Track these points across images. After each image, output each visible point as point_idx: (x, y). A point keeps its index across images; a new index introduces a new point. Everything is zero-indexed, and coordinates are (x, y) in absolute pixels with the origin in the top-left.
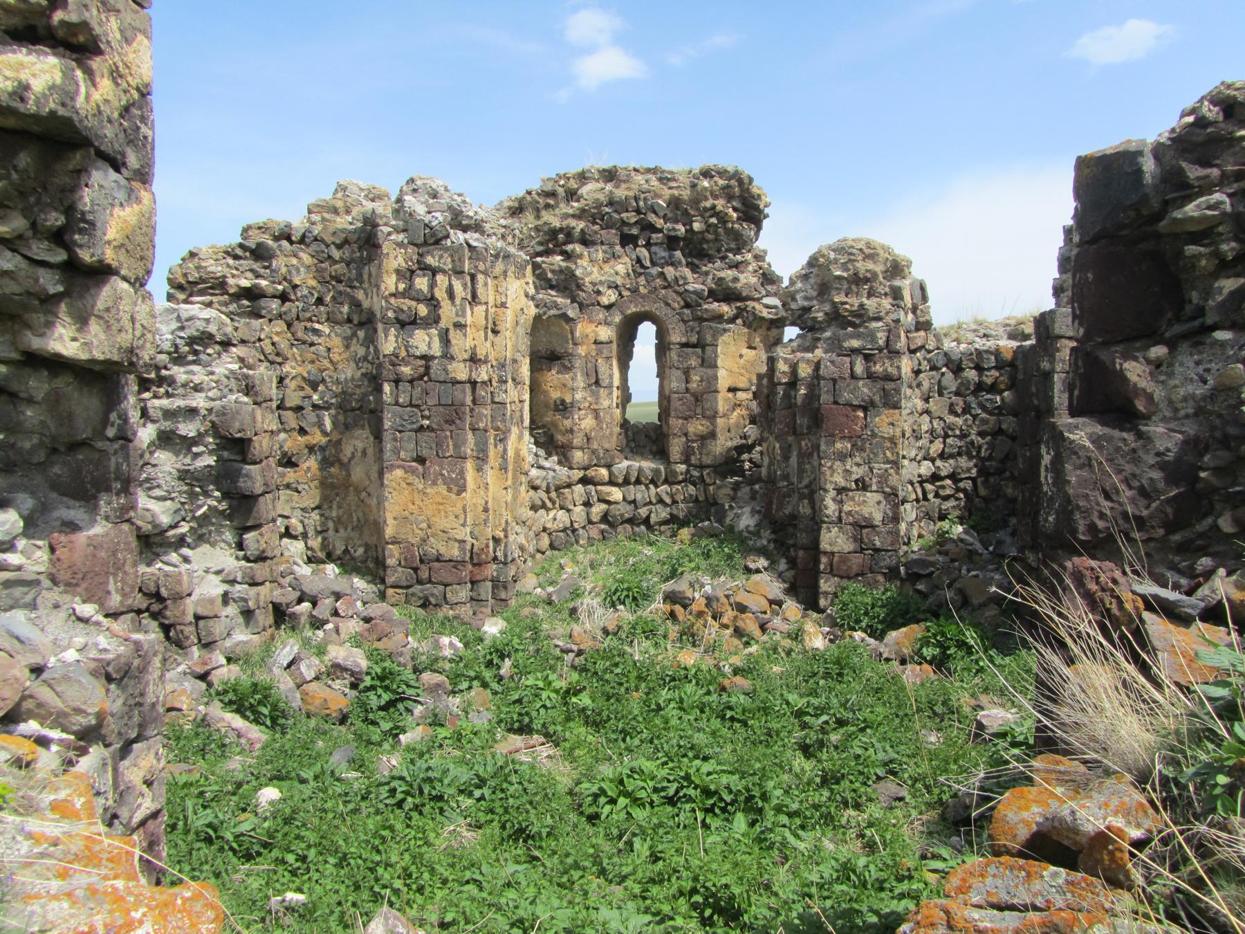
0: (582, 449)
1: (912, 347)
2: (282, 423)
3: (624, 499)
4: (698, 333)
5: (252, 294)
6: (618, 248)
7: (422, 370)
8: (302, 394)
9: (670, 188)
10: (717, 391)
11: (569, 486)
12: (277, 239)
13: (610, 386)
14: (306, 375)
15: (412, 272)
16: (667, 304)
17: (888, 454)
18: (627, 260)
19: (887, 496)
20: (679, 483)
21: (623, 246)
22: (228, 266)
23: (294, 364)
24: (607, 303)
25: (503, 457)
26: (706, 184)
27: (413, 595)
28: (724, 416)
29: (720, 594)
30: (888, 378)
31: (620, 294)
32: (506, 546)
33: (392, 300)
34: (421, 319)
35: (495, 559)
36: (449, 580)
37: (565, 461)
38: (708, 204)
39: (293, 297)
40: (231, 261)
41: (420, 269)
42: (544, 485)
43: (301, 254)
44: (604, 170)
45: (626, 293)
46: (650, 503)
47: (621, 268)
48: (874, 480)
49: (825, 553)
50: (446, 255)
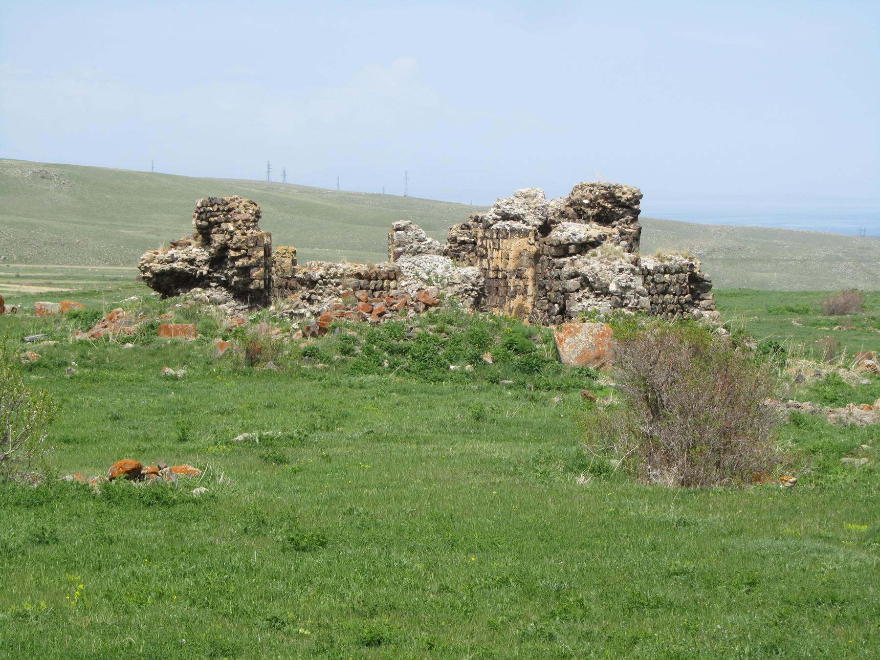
22: (458, 232)
40: (460, 231)
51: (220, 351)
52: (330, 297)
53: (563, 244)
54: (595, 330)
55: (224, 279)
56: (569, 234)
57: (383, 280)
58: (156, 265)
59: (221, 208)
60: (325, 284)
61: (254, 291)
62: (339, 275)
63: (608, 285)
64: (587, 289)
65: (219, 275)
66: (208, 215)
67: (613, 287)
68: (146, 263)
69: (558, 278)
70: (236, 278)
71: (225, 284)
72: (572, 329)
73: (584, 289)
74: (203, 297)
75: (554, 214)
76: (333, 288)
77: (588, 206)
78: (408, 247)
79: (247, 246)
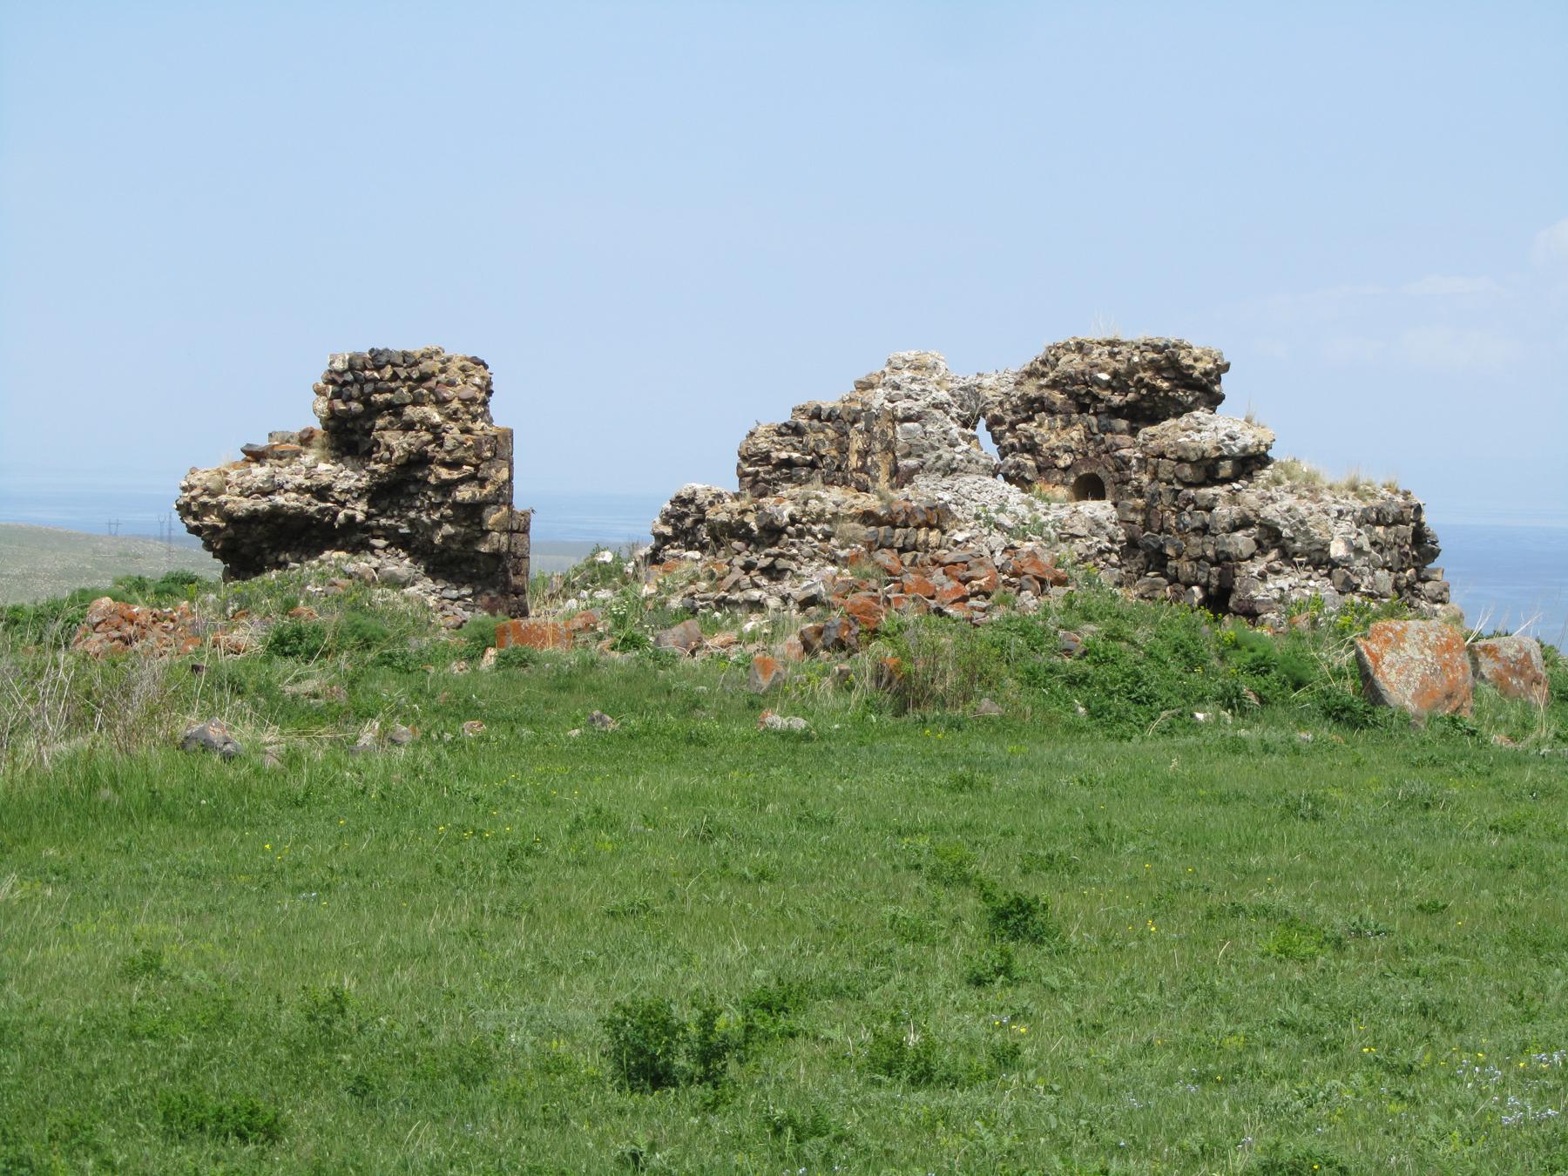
5: (788, 463)
6: (1075, 416)
21: (1079, 413)
22: (773, 442)
40: (776, 439)
43: (827, 430)
47: (1075, 434)
51: (761, 677)
52: (815, 564)
53: (1208, 458)
54: (1432, 637)
55: (405, 530)
56: (1221, 435)
57: (918, 527)
58: (235, 498)
59: (403, 374)
60: (800, 534)
61: (481, 558)
62: (829, 516)
63: (1327, 545)
64: (1273, 554)
65: (392, 522)
66: (368, 388)
67: (1337, 550)
68: (202, 495)
69: (1204, 530)
70: (448, 529)
71: (412, 544)
72: (1391, 635)
73: (1265, 553)
74: (366, 571)
75: (1001, 403)
76: (816, 543)
77: (1108, 385)
78: (930, 457)
79: (478, 457)
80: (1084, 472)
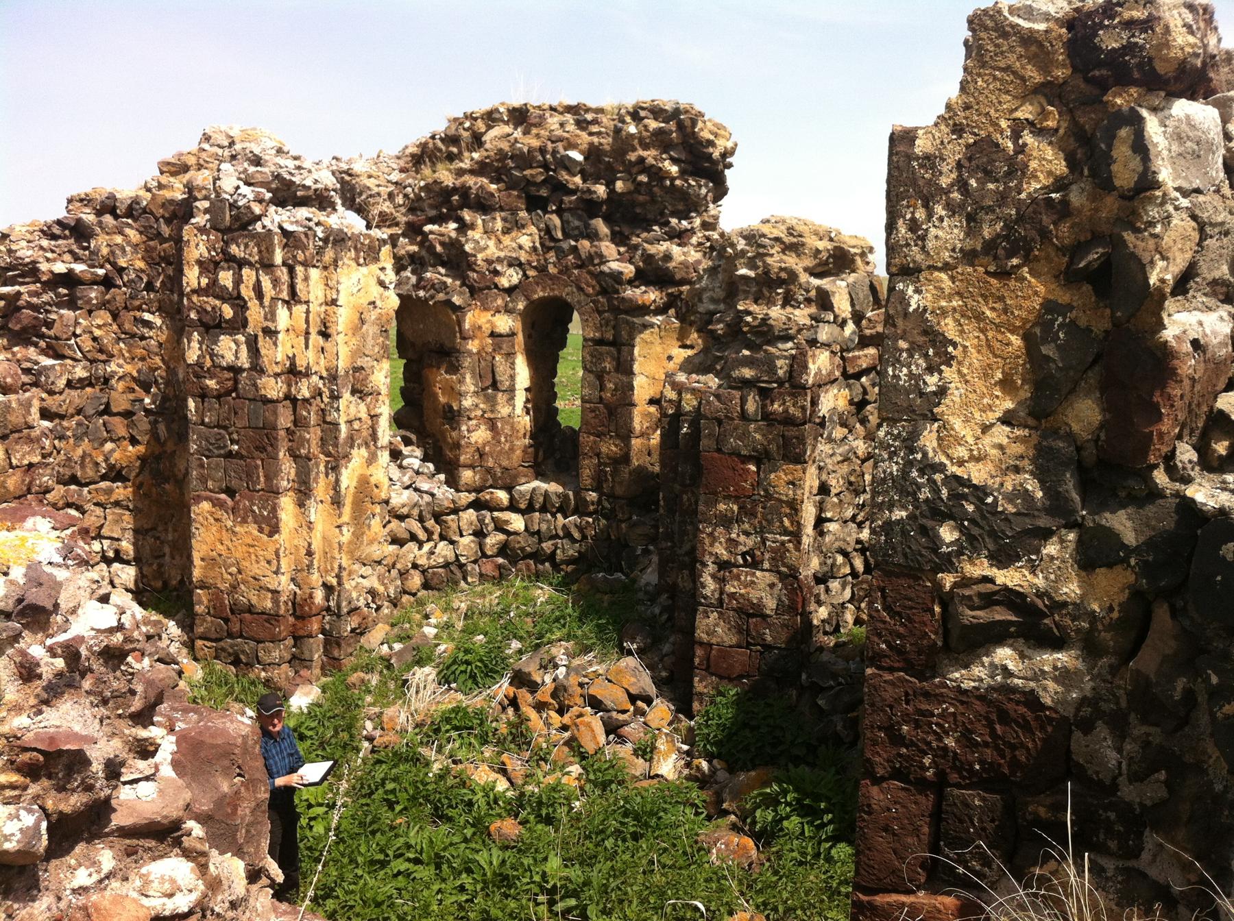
0: (471, 467)
1: (851, 371)
2: (108, 432)
3: (527, 529)
4: (614, 328)
5: (69, 279)
6: (523, 214)
7: (230, 384)
8: (131, 396)
9: (591, 134)
10: (634, 405)
11: (455, 511)
12: (99, 213)
13: (511, 390)
14: (135, 374)
15: (217, 264)
16: (580, 289)
17: (787, 522)
18: (533, 229)
19: (782, 577)
20: (590, 515)
21: (529, 210)
22: (42, 248)
23: (121, 361)
24: (507, 285)
25: (335, 489)
26: (632, 129)
27: (223, 649)
28: (642, 435)
29: (573, 681)
30: (788, 421)
31: (525, 274)
32: (339, 596)
33: (195, 298)
34: (227, 321)
35: (328, 609)
36: (262, 636)
37: (452, 482)
38: (632, 157)
39: (119, 282)
40: (45, 243)
41: (227, 261)
42: (415, 512)
43: (128, 231)
44: (515, 109)
45: (531, 273)
46: (557, 536)
47: (525, 241)
48: (767, 556)
49: (701, 644)
50: (251, 244)
75: (391, 196)
80: (540, 294)
